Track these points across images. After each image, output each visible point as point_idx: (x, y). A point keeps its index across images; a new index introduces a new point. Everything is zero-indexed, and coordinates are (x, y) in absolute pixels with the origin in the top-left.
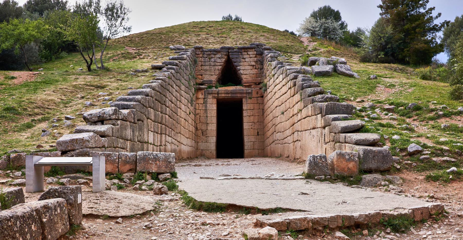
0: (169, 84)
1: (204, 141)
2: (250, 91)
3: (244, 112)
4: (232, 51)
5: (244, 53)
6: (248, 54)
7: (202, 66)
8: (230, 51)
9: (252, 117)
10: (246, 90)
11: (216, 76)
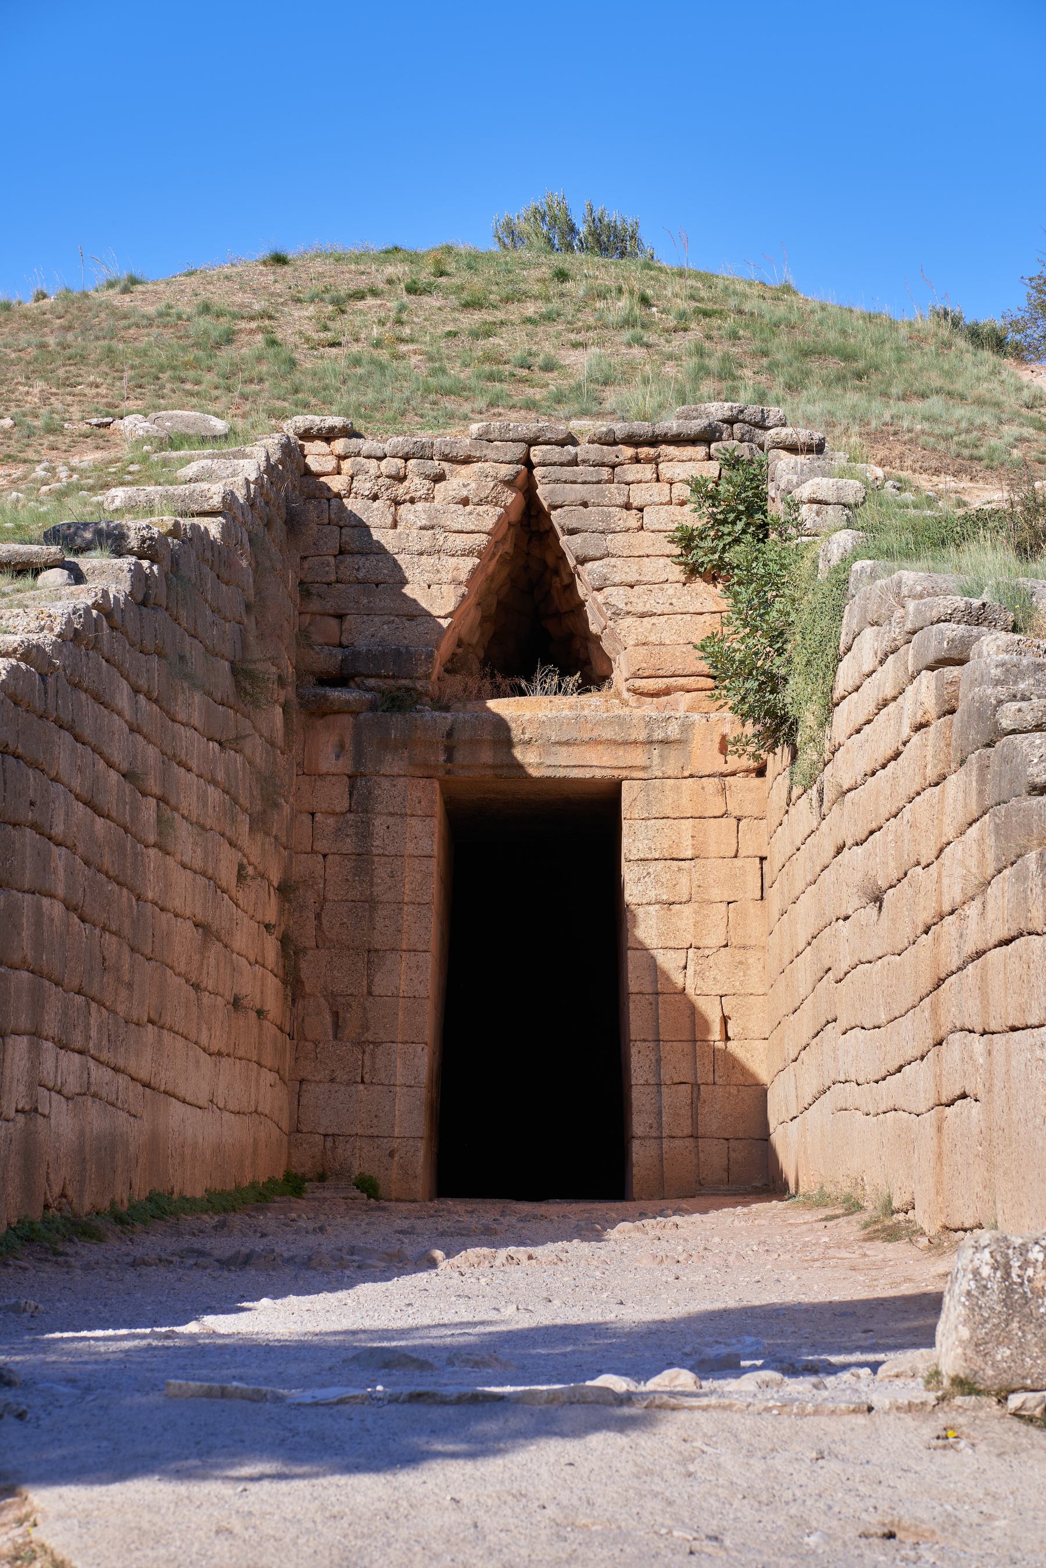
0: (76, 686)
1: (342, 1076)
2: (673, 731)
4: (555, 453)
5: (632, 472)
6: (658, 480)
8: (537, 453)
9: (687, 910)
10: (649, 722)
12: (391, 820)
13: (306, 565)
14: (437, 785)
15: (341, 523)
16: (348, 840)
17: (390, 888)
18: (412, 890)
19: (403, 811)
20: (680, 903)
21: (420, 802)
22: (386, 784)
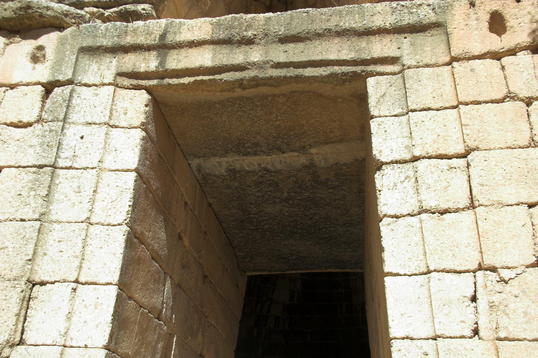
3: (383, 180)
12: (86, 130)
16: (31, 151)
19: (102, 121)
20: (457, 211)
21: (126, 114)
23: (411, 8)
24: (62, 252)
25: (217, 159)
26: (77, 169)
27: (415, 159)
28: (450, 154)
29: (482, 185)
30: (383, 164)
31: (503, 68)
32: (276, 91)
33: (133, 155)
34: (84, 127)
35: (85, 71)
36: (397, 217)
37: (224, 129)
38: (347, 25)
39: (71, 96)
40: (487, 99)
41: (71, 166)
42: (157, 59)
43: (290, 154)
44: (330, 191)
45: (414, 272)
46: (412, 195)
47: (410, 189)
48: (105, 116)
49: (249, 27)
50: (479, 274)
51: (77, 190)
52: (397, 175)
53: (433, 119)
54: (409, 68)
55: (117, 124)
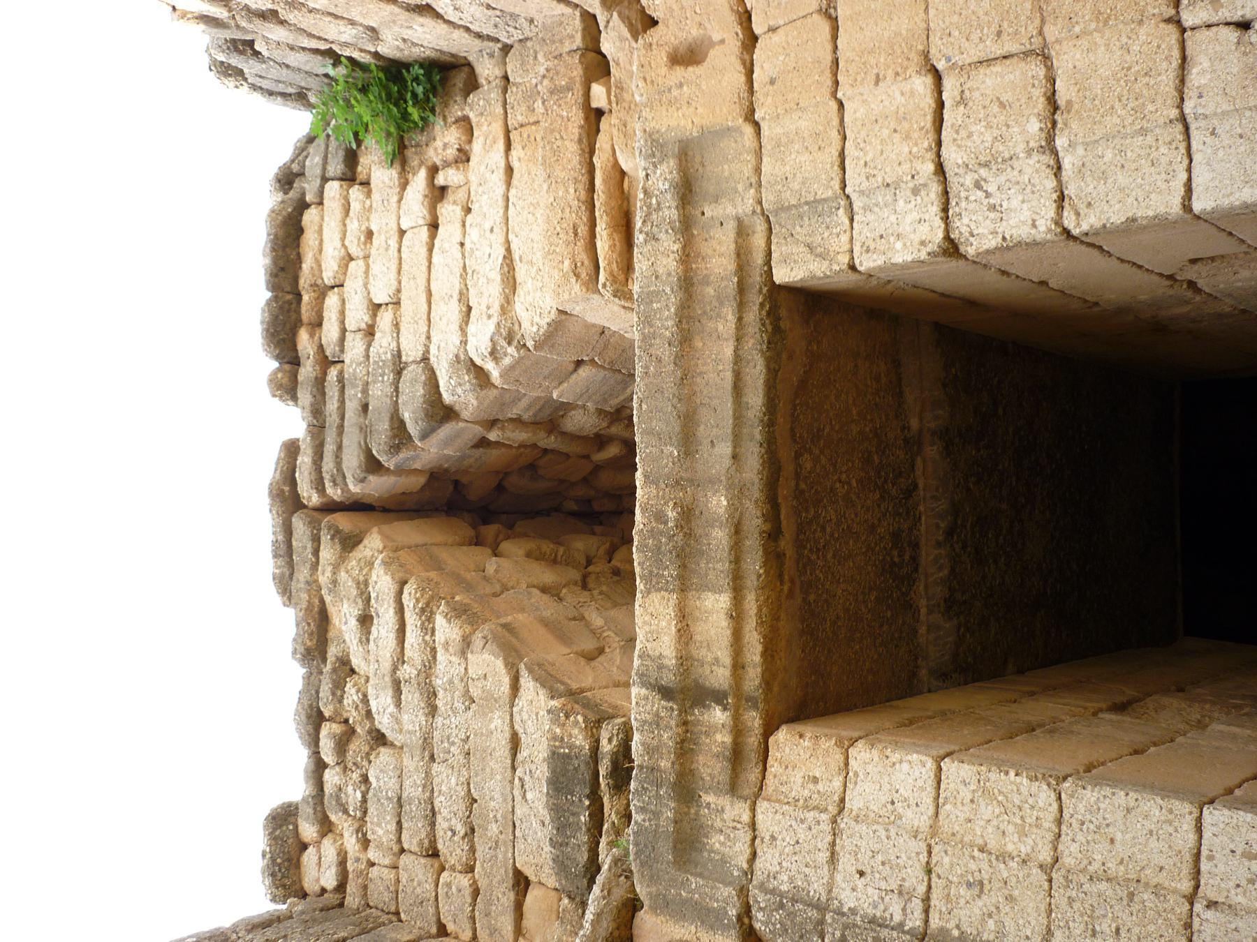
2: (662, 179)
3: (981, 232)
4: (305, 460)
5: (330, 332)
7: (435, 854)
9: (1067, 59)
11: (527, 683)
12: (846, 864)
13: (450, 927)
14: (782, 735)
15: (396, 848)
17: (1010, 899)
18: (1022, 833)
19: (827, 827)
21: (815, 780)
22: (767, 861)
23: (649, 206)
24: (1118, 930)
25: (923, 630)
26: (929, 887)
27: (940, 170)
28: (934, 105)
29: (999, 34)
30: (947, 238)
31: (772, 30)
32: (788, 469)
33: (905, 766)
34: (840, 868)
35: (724, 861)
36: (1062, 197)
37: (861, 598)
38: (670, 323)
39: (773, 892)
40: (829, 47)
41: (923, 901)
42: (709, 707)
43: (919, 472)
44: (1000, 411)
45: (1183, 151)
46: (1016, 173)
47: (1002, 179)
48: (818, 823)
49: (660, 517)
50: (1188, 19)
51: (977, 890)
52: (972, 206)
53: (862, 145)
54: (760, 203)
55: (836, 798)
